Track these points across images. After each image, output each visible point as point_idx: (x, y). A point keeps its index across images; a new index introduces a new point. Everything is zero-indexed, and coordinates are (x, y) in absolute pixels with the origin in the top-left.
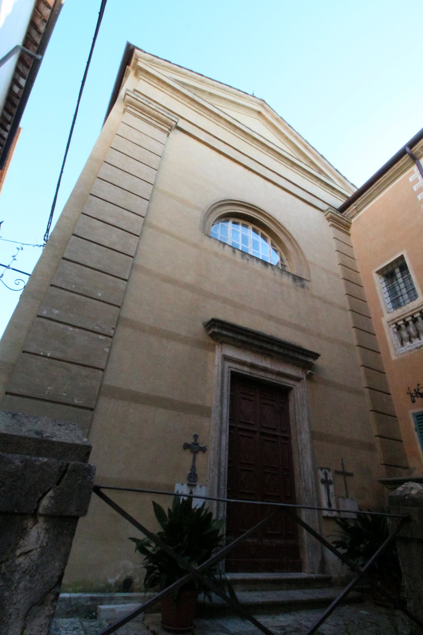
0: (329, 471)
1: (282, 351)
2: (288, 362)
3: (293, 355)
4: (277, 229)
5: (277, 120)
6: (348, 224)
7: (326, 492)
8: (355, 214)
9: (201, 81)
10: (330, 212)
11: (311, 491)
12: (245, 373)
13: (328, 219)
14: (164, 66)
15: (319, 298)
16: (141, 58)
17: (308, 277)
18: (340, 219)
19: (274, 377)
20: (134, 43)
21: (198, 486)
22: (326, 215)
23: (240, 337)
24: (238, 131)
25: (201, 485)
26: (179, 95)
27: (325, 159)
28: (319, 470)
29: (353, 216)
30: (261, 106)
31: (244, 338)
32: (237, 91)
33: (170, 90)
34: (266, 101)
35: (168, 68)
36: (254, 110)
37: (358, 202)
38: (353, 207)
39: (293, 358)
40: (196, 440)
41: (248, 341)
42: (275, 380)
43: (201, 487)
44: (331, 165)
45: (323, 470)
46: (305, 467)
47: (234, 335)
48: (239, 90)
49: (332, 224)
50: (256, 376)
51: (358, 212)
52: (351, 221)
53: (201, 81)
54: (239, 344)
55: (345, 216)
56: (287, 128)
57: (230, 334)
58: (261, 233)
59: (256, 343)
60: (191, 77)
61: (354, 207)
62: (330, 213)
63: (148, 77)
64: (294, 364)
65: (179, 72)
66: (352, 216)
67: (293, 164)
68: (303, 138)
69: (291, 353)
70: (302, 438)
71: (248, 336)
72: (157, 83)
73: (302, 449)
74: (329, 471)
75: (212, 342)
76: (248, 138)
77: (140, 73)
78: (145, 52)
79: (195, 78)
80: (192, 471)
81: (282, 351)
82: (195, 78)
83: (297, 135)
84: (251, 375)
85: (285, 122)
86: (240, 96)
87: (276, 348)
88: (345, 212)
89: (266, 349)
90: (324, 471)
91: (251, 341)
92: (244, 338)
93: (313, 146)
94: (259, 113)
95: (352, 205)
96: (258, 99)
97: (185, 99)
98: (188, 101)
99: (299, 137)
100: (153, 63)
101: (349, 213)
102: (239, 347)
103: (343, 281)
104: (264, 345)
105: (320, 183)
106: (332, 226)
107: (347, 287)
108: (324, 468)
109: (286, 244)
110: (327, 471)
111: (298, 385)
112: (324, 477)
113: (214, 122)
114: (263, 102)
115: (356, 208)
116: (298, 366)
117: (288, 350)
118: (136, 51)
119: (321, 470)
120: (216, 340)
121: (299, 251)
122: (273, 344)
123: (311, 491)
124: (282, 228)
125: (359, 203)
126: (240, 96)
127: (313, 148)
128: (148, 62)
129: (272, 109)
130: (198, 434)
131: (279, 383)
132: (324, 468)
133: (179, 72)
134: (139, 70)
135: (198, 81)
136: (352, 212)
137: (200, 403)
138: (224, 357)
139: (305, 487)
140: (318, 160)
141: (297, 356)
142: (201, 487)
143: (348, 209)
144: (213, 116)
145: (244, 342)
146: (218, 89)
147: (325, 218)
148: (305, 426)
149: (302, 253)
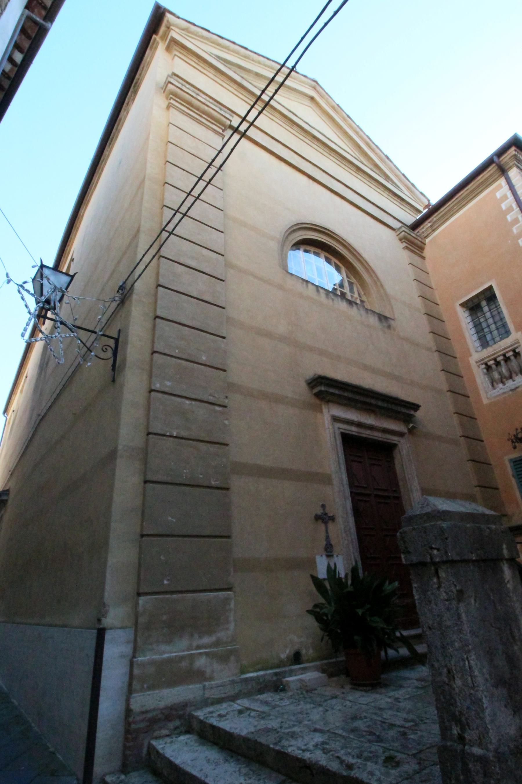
5: (333, 108)
6: (422, 245)
8: (430, 233)
9: (246, 57)
10: (404, 231)
12: (354, 433)
13: (401, 240)
14: (202, 37)
16: (174, 25)
18: (414, 239)
21: (335, 556)
22: (397, 235)
23: (346, 394)
24: (295, 128)
25: (337, 554)
26: (223, 78)
27: (391, 161)
29: (428, 235)
30: (313, 89)
31: (350, 395)
34: (319, 82)
35: (207, 39)
37: (433, 219)
40: (324, 509)
43: (337, 556)
49: (406, 247)
50: (364, 436)
51: (434, 231)
52: (425, 241)
55: (418, 234)
58: (335, 263)
61: (429, 225)
62: (403, 233)
65: (219, 45)
66: (426, 235)
67: (359, 169)
68: (364, 134)
72: (196, 61)
75: (318, 401)
77: (175, 47)
79: (238, 53)
82: (238, 53)
83: (358, 130)
87: (380, 403)
89: (370, 404)
92: (350, 395)
94: (312, 98)
95: (427, 222)
97: (232, 84)
98: (235, 86)
99: (361, 133)
100: (189, 32)
102: (345, 405)
103: (425, 317)
105: (387, 193)
107: (430, 323)
109: (364, 275)
115: (431, 226)
118: (168, 15)
125: (435, 219)
127: (377, 146)
129: (327, 93)
130: (324, 504)
134: (173, 43)
135: (242, 56)
142: (337, 556)
143: (422, 227)
145: (349, 399)
147: (397, 238)
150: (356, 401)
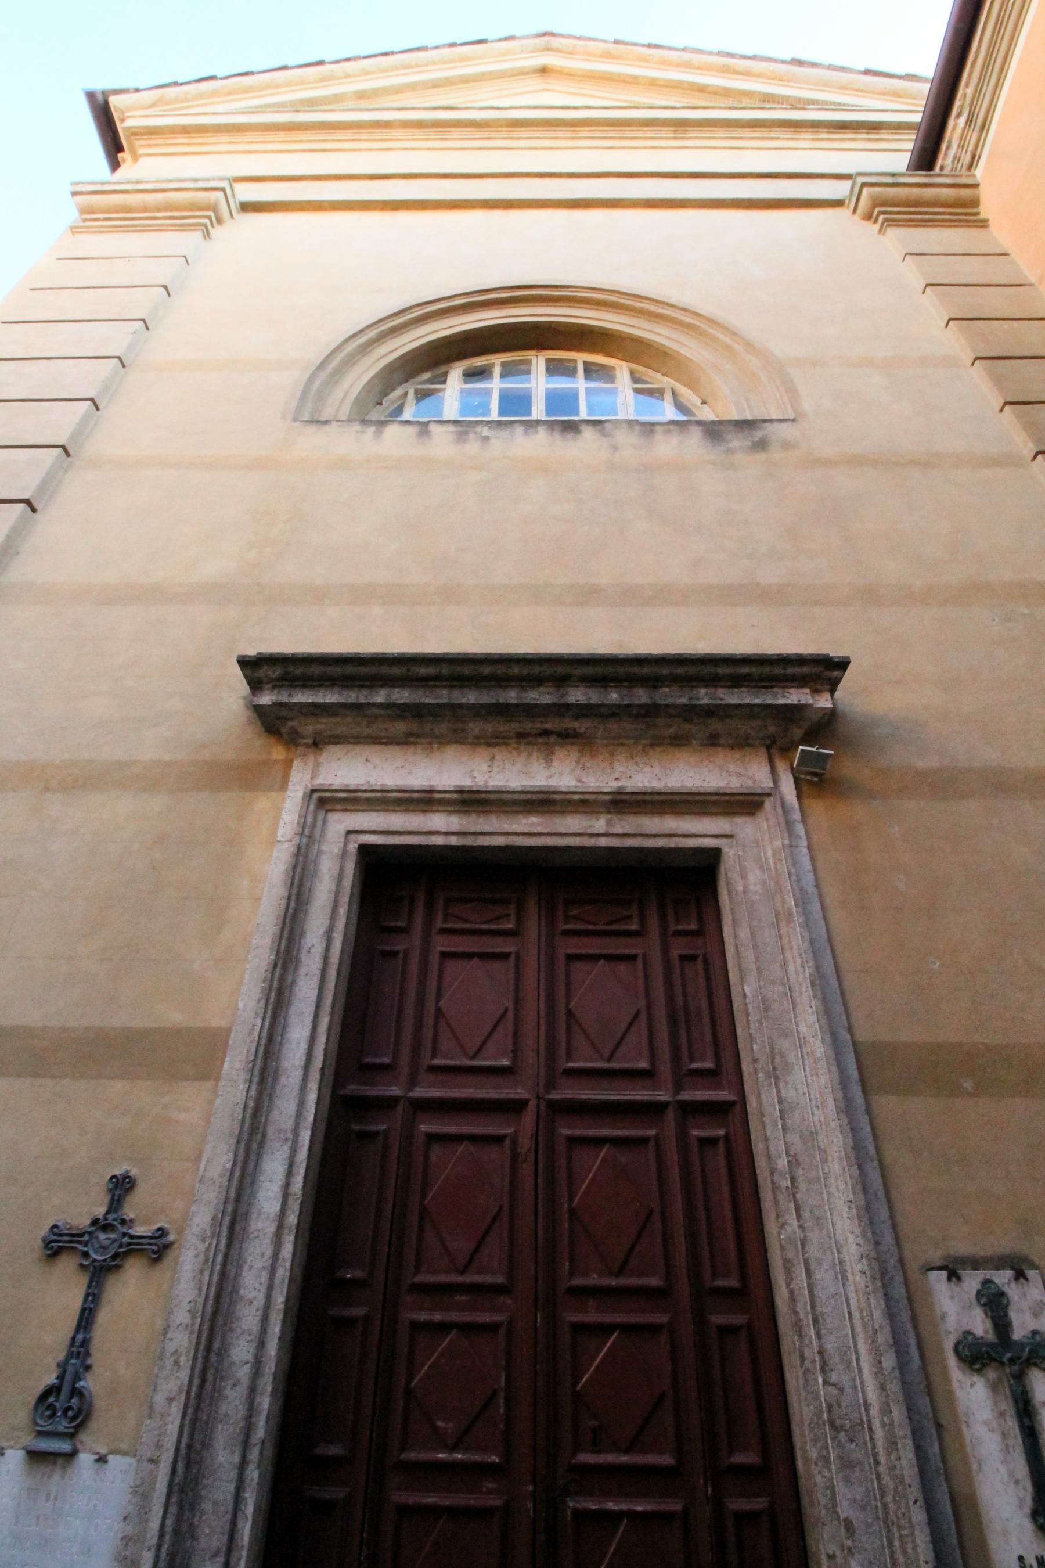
0: (1020, 1275)
1: (614, 696)
2: (679, 741)
3: (684, 700)
4: (634, 321)
5: (607, 56)
6: (965, 193)
7: (1012, 1424)
8: (978, 141)
9: (324, 79)
10: (864, 185)
11: (879, 1433)
12: (438, 841)
13: (868, 217)
14: (201, 96)
15: (856, 461)
16: (129, 109)
17: (790, 410)
18: (916, 191)
19: (600, 824)
20: (99, 84)
21: (85, 1459)
22: (855, 211)
23: (380, 697)
24: (456, 133)
25: (103, 1451)
26: (250, 136)
27: (814, 65)
28: (938, 1279)
29: (973, 157)
30: (546, 52)
31: (403, 696)
32: (446, 51)
33: (224, 138)
34: (555, 31)
35: (214, 93)
36: (522, 73)
37: (965, 96)
38: (955, 125)
39: (691, 713)
40: (115, 1203)
41: (427, 701)
42: (607, 835)
43: (102, 1460)
44: (843, 69)
45: (961, 1272)
46: (823, 1276)
47: (352, 696)
48: (453, 45)
49: (886, 220)
50: (499, 841)
51: (984, 127)
52: (974, 176)
53: (324, 79)
54: (400, 727)
55: (945, 172)
56: (645, 60)
57: (329, 697)
58: (587, 365)
59: (471, 697)
60: (288, 84)
61: (962, 120)
62: (865, 190)
63: (160, 141)
64: (713, 741)
65: (248, 90)
66: (966, 159)
67: (681, 125)
68: (710, 53)
69: (672, 696)
70: (788, 1093)
71: (423, 682)
72: (185, 141)
73: (794, 1162)
74: (1020, 1275)
75: (278, 753)
76: (492, 135)
77: (137, 143)
78: (137, 90)
79: (302, 82)
80: (61, 1377)
81: (614, 696)
82: (302, 82)
83: (686, 56)
84: (469, 841)
85: (635, 44)
86: (464, 59)
87: (577, 695)
88: (939, 163)
89: (531, 711)
90: (972, 1281)
91: (443, 696)
92: (403, 696)
93: (750, 54)
94: (544, 71)
95: (951, 123)
96: (527, 37)
97: (271, 136)
98: (281, 136)
99: (696, 58)
100: (169, 103)
101: (955, 158)
102: (405, 741)
103: (978, 374)
104: (511, 696)
105: (809, 136)
106: (889, 226)
107: (998, 381)
108: (976, 1263)
109: (683, 351)
110: (1003, 1278)
111: (745, 827)
112: (980, 1325)
113: (370, 150)
114: (547, 38)
115: (969, 122)
116: (741, 744)
117: (653, 682)
118: (113, 101)
119: (953, 1275)
120: (292, 740)
121: (738, 347)
122: (562, 681)
123: (879, 1433)
124: (652, 308)
125: (970, 92)
126: (464, 59)
127: (753, 58)
128: (151, 110)
129: (579, 38)
130: (134, 1172)
131: (630, 843)
132: (976, 1263)
133: (248, 90)
134: (132, 138)
135: (316, 82)
136: (961, 146)
137: (175, 1017)
138: (316, 795)
139: (830, 1407)
140: (788, 81)
141: (704, 696)
142: (102, 1460)
143: (944, 146)
144: (364, 134)
145: (415, 712)
146: (385, 74)
147: (857, 218)
148: (803, 1029)
149: (749, 346)
150: (434, 712)
